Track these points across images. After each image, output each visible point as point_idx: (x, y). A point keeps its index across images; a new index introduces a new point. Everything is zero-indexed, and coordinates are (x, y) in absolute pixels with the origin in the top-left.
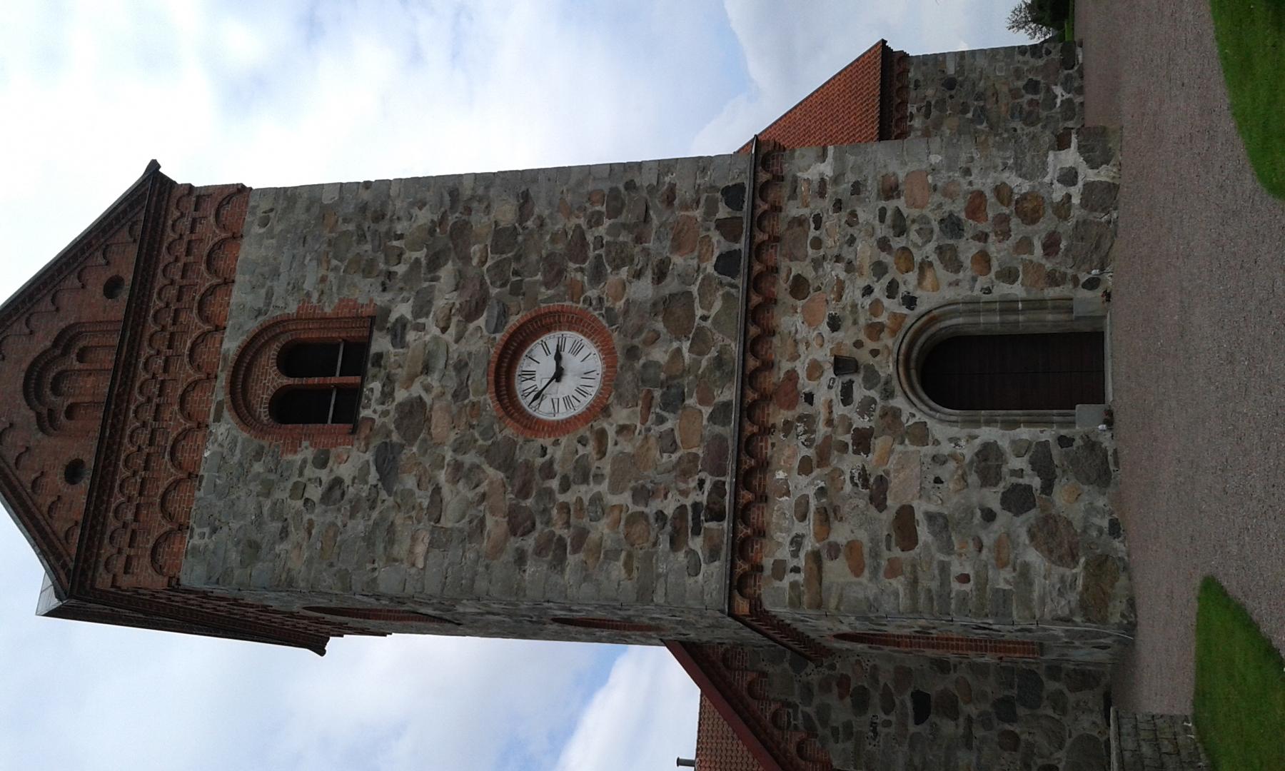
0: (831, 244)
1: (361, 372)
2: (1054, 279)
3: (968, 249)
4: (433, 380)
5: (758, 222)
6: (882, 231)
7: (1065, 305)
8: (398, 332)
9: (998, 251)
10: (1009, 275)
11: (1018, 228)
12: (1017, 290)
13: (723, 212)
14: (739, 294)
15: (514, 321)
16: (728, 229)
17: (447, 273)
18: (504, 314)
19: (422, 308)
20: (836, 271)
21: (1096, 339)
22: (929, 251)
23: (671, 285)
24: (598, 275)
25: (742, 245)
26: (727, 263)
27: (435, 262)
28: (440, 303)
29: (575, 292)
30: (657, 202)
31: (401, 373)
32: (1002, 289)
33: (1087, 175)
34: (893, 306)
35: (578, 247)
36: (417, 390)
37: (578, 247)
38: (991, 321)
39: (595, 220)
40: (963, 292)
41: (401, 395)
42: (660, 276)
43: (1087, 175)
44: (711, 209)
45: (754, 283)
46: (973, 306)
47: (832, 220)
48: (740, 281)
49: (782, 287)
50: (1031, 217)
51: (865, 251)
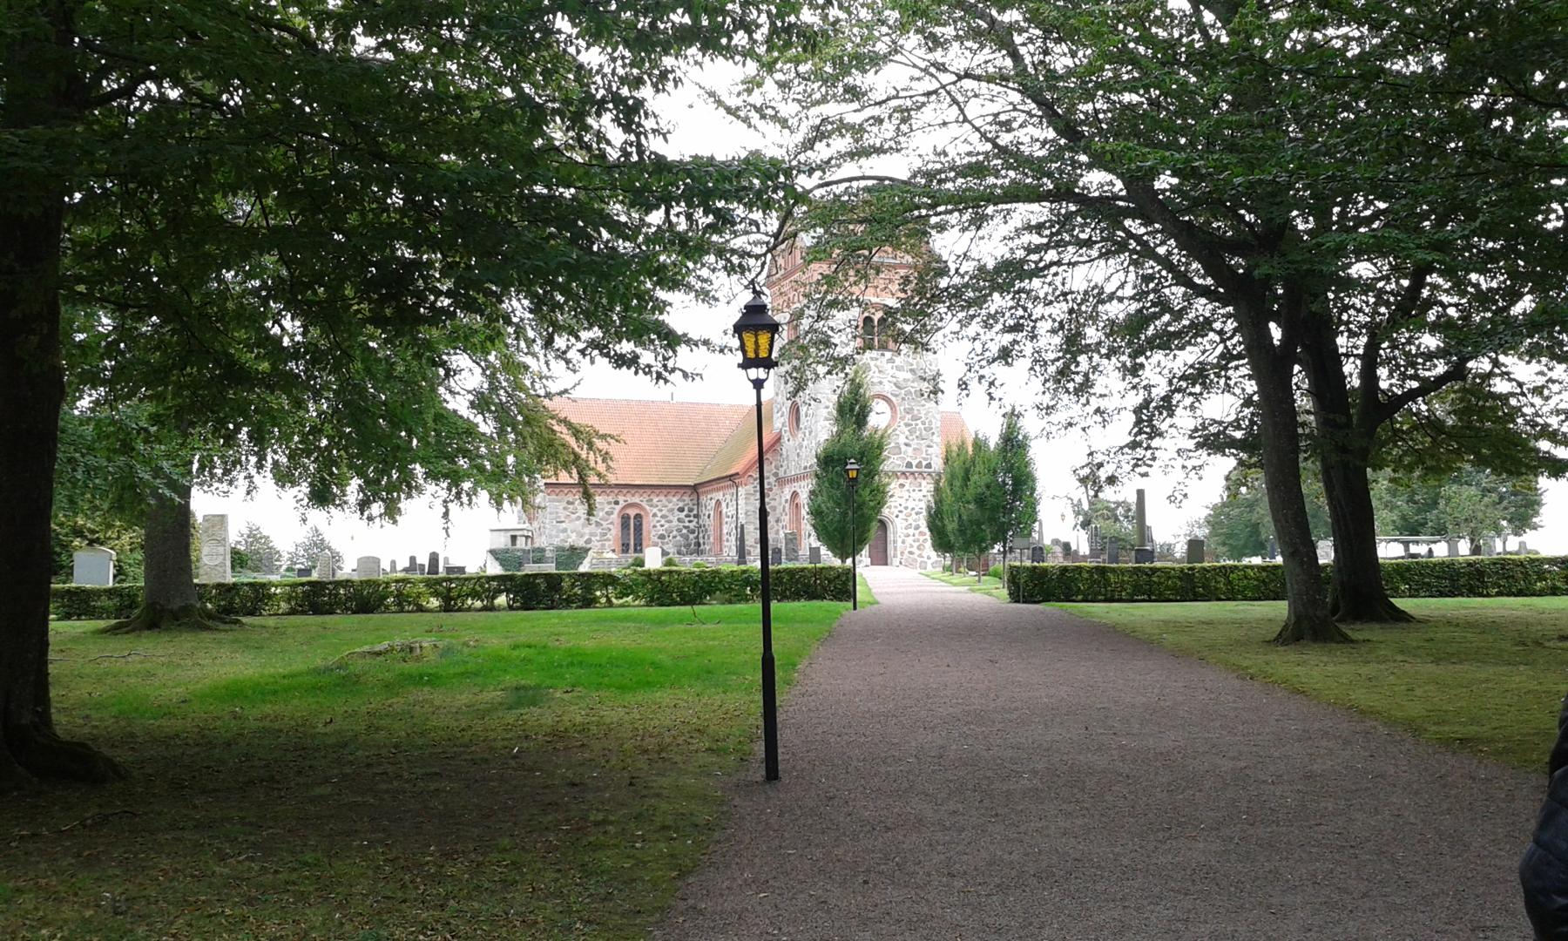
0: (913, 494)
1: (879, 349)
2: (902, 553)
3: (911, 531)
4: (877, 374)
5: (920, 473)
6: (917, 510)
7: (895, 556)
8: (891, 361)
9: (911, 538)
10: (903, 542)
11: (916, 544)
12: (899, 544)
13: (924, 463)
14: (901, 469)
15: (893, 399)
16: (919, 465)
17: (909, 376)
18: (896, 396)
19: (899, 368)
20: (906, 495)
21: (886, 564)
22: (910, 520)
23: (903, 448)
24: (907, 425)
25: (914, 469)
26: (909, 465)
27: (912, 371)
28: (898, 374)
29: (902, 418)
30: (928, 442)
31: (878, 363)
32: (900, 541)
33: (929, 562)
34: (896, 513)
35: (915, 418)
36: (873, 368)
37: (915, 418)
38: (891, 537)
39: (923, 423)
40: (899, 530)
41: (872, 363)
42: (906, 445)
43: (929, 562)
44: (925, 459)
45: (903, 473)
46: (895, 533)
47: (921, 494)
48: (904, 469)
49: (902, 481)
50: (918, 548)
51: (911, 504)
